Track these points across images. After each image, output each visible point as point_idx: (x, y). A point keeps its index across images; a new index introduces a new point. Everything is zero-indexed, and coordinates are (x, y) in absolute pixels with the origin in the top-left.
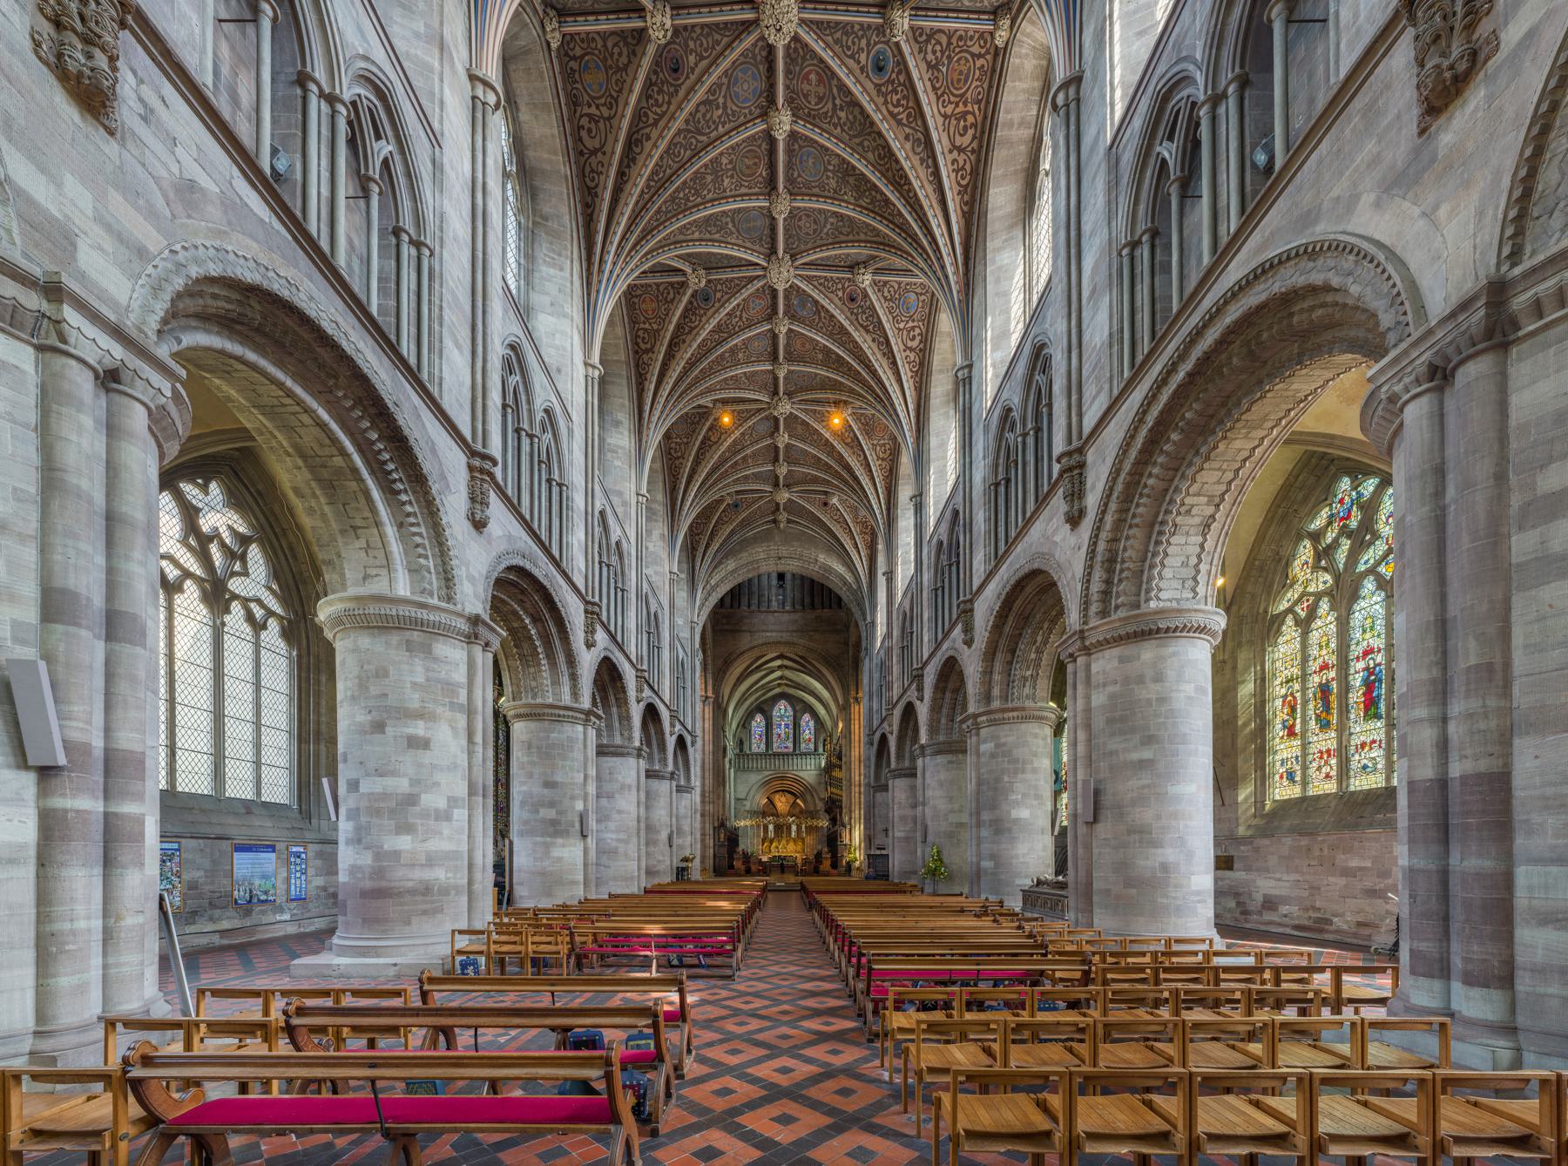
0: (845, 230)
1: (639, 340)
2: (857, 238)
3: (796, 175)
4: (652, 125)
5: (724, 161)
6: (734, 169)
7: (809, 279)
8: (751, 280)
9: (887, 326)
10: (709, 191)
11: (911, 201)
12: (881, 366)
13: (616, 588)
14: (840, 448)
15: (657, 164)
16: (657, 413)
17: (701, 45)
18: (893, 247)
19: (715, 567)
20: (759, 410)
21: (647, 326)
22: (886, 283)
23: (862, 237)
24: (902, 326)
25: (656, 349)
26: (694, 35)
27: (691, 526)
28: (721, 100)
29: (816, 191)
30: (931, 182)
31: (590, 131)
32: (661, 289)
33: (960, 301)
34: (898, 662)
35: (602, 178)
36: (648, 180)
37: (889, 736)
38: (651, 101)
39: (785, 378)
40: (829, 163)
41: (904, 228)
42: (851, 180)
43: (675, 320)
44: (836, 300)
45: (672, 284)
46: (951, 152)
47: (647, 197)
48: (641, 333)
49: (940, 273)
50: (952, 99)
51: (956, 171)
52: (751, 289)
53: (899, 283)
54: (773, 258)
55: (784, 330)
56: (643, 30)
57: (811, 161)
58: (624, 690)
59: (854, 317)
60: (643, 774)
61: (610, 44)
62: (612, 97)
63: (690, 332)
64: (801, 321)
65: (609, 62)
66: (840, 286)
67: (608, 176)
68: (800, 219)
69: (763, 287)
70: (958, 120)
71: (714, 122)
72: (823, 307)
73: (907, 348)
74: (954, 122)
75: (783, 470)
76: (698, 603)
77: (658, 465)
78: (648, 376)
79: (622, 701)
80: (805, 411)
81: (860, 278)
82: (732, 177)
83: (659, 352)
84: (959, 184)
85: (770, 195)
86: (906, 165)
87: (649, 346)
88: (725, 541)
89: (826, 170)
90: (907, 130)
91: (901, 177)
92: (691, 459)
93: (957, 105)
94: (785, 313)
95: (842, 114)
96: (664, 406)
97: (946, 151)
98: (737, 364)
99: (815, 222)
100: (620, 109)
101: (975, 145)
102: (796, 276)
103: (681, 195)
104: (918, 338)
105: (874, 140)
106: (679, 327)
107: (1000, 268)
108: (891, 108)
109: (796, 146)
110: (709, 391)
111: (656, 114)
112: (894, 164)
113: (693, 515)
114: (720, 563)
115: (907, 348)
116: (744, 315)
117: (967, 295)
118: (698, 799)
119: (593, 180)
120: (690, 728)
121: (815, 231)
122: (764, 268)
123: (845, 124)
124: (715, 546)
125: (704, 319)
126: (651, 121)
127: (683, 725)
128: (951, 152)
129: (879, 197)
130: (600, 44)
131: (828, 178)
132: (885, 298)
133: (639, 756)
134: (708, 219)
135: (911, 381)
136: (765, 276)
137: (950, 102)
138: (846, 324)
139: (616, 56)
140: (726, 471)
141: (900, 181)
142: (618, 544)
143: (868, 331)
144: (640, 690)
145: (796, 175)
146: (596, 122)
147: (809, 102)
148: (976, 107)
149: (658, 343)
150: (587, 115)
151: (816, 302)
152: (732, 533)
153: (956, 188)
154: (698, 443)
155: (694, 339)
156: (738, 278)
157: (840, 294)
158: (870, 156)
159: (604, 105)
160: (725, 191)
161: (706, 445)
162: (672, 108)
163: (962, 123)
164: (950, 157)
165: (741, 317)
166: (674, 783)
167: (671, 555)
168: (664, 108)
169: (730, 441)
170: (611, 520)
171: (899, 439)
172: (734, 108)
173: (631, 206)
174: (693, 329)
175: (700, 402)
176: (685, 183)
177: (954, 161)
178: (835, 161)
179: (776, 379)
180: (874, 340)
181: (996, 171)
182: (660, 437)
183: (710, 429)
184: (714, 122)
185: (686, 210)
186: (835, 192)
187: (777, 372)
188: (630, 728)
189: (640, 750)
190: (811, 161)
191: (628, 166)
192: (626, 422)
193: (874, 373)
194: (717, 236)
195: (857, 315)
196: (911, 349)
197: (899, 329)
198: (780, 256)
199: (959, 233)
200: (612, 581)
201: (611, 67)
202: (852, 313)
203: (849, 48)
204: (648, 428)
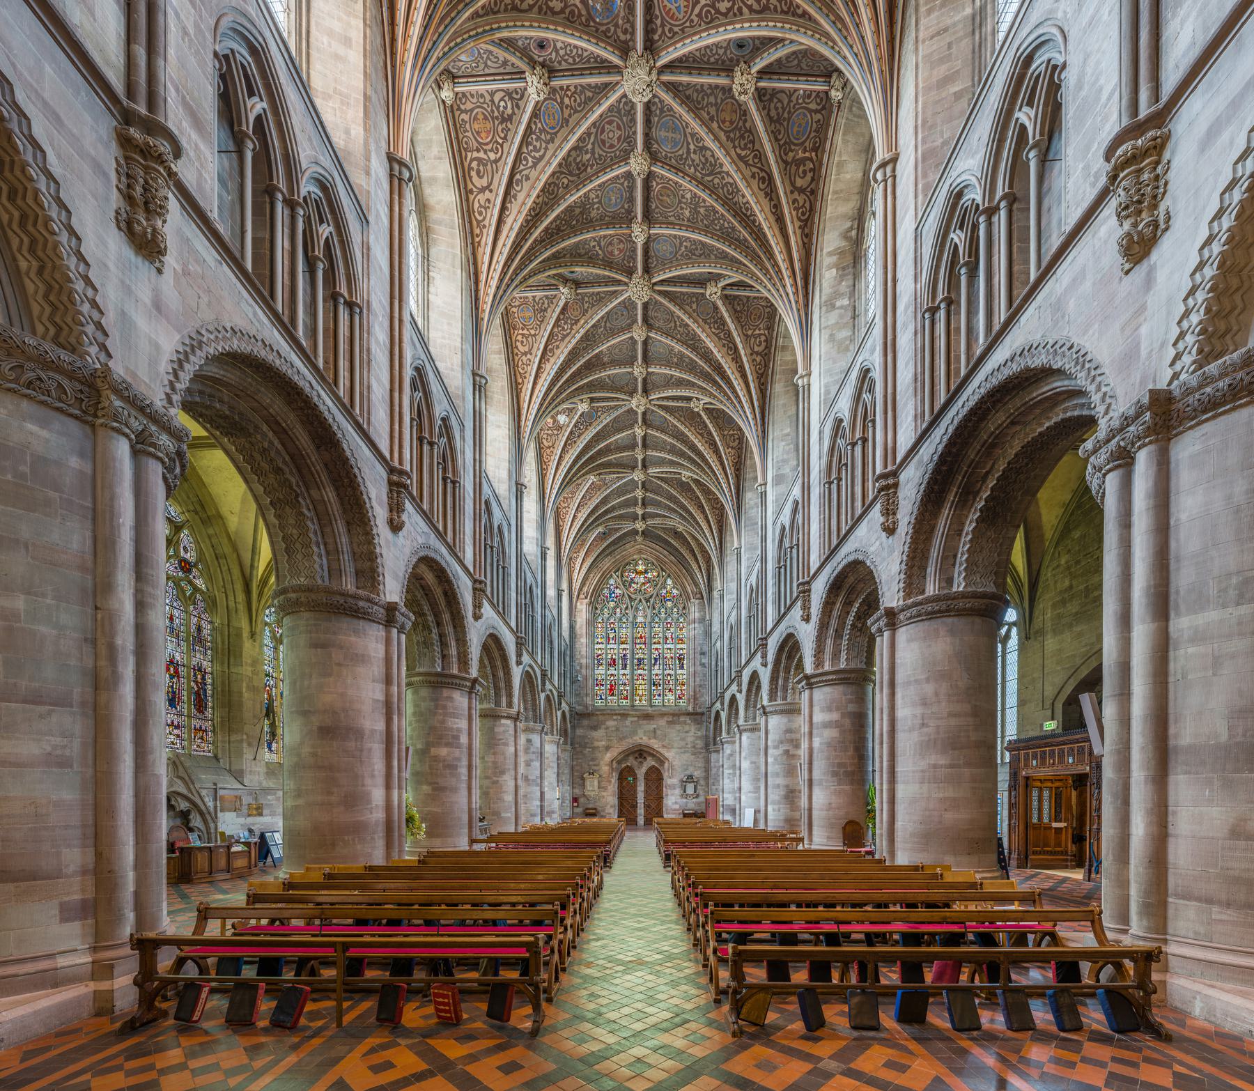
21: (525, 332)
24: (750, 332)
31: (478, 172)
38: (531, 148)
45: (547, 297)
48: (519, 338)
61: (496, 99)
63: (563, 339)
70: (798, 166)
74: (794, 168)
84: (799, 219)
104: (764, 344)
111: (534, 157)
128: (792, 192)
130: (488, 98)
150: (476, 159)
157: (694, 306)
159: (491, 150)
168: (541, 153)
177: (795, 201)
196: (758, 353)
197: (747, 336)
199: (800, 260)
201: (497, 118)
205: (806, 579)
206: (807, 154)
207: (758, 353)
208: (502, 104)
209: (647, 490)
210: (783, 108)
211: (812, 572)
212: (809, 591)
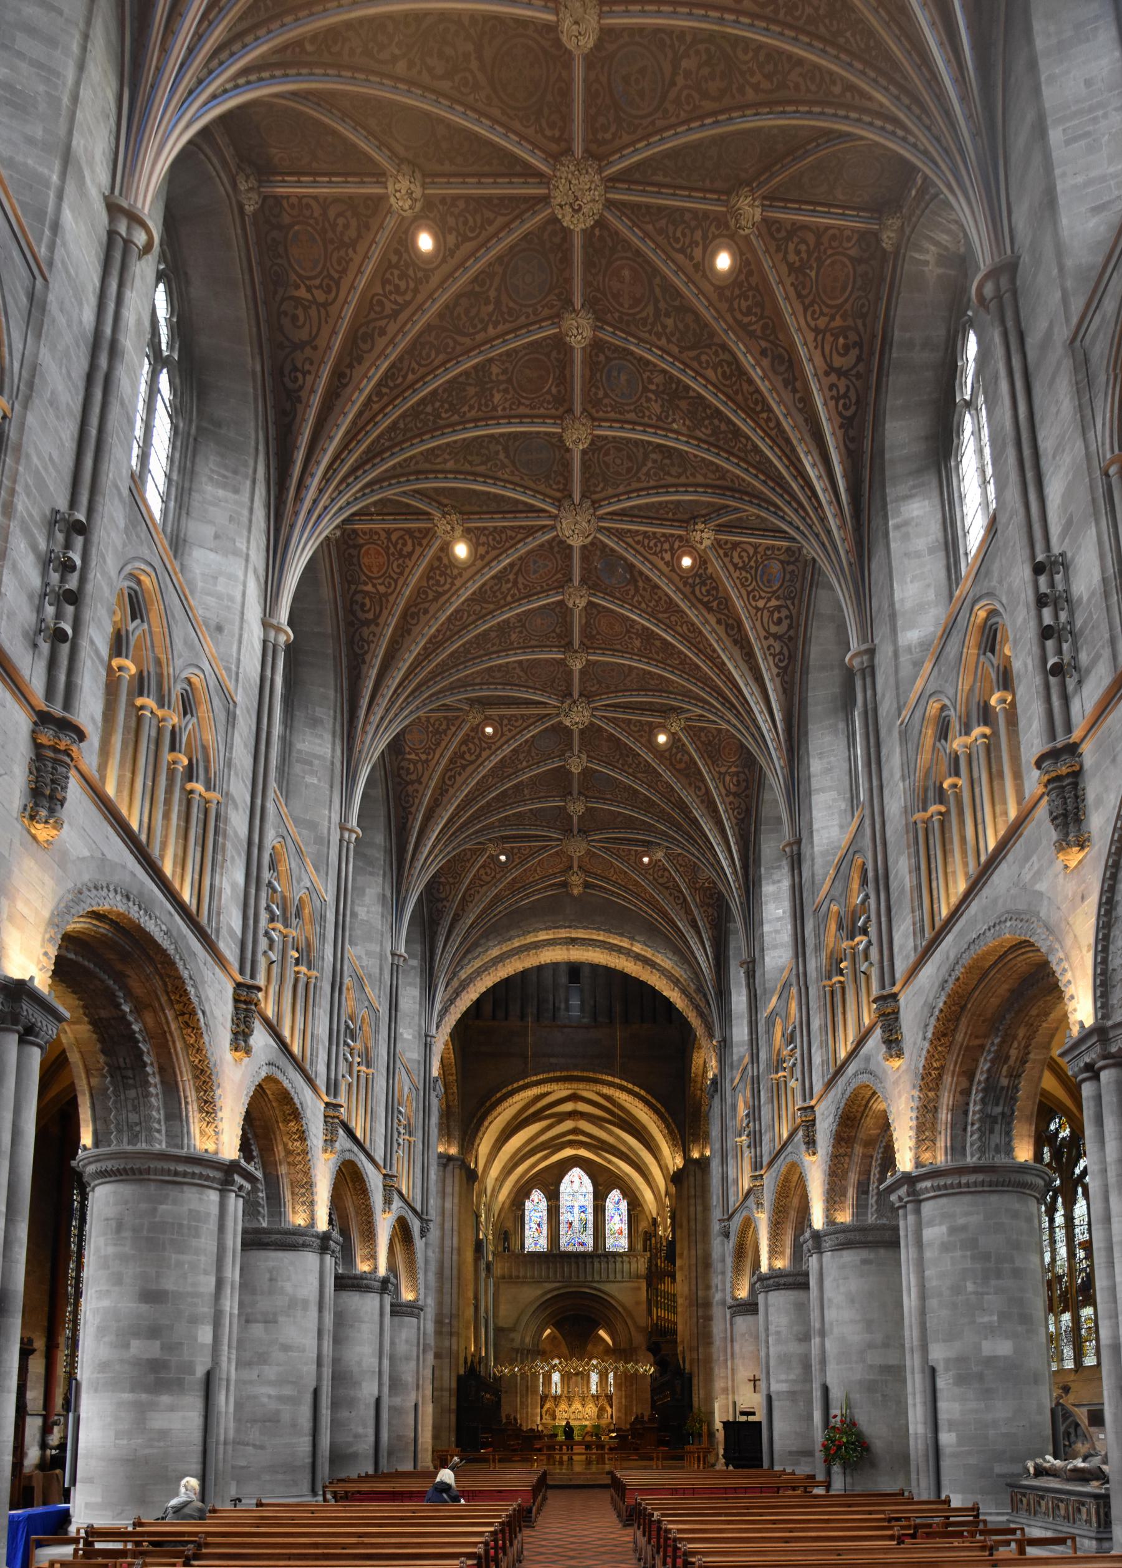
0: (674, 471)
1: (356, 607)
2: (692, 480)
3: (601, 394)
4: (389, 317)
5: (495, 370)
6: (509, 381)
7: (619, 535)
8: (532, 531)
9: (738, 604)
10: (471, 408)
11: (773, 433)
12: (731, 658)
14: (667, 776)
15: (393, 366)
16: (379, 712)
17: (466, 223)
18: (747, 493)
19: (468, 951)
20: (542, 718)
22: (735, 545)
23: (700, 479)
25: (381, 620)
26: (456, 211)
27: (429, 886)
28: (492, 294)
29: (631, 416)
30: (800, 410)
32: (394, 537)
33: (850, 564)
35: (309, 379)
36: (379, 384)
38: (388, 288)
39: (583, 672)
40: (650, 381)
41: (764, 468)
42: (683, 405)
43: (413, 580)
44: (661, 565)
45: (409, 531)
46: (827, 374)
47: (376, 407)
49: (818, 528)
50: (825, 310)
51: (837, 399)
52: (532, 543)
53: (756, 547)
54: (566, 503)
55: (582, 603)
56: (382, 199)
57: (623, 378)
59: (687, 590)
61: (332, 213)
62: (332, 278)
63: (436, 599)
64: (608, 593)
65: (330, 235)
66: (666, 546)
67: (317, 376)
68: (607, 454)
69: (550, 542)
70: (836, 337)
71: (482, 321)
72: (641, 573)
73: (769, 635)
74: (829, 338)
75: (577, 808)
76: (438, 1007)
77: (379, 792)
78: (368, 658)
80: (613, 720)
81: (697, 536)
82: (506, 391)
83: (386, 624)
84: (840, 414)
85: (561, 418)
86: (764, 386)
87: (370, 616)
88: (484, 911)
89: (646, 389)
90: (764, 344)
91: (756, 403)
92: (433, 784)
93: (833, 318)
94: (583, 581)
95: (669, 322)
96: (392, 702)
97: (820, 373)
98: (508, 649)
99: (629, 458)
100: (342, 295)
101: (861, 368)
102: (600, 529)
103: (429, 409)
104: (786, 623)
105: (716, 354)
106: (419, 591)
107: (906, 523)
108: (739, 316)
109: (602, 358)
110: (463, 684)
111: (396, 302)
112: (745, 386)
113: (432, 871)
114: (476, 945)
115: (769, 635)
116: (520, 580)
117: (860, 556)
118: (430, 1327)
119: (296, 380)
120: (419, 1208)
121: (629, 470)
122: (555, 517)
123: (673, 334)
125: (458, 583)
126: (388, 311)
128: (827, 374)
129: (723, 427)
130: (317, 212)
131: (648, 400)
132: (735, 566)
134: (467, 444)
135: (778, 680)
136: (553, 527)
137: (822, 314)
138: (677, 598)
139: (339, 229)
140: (488, 804)
141: (756, 407)
143: (710, 609)
145: (601, 394)
146: (306, 309)
147: (622, 305)
148: (859, 322)
149: (385, 612)
151: (631, 567)
153: (838, 420)
154: (444, 762)
155: (441, 608)
156: (512, 528)
157: (667, 556)
158: (710, 373)
159: (320, 287)
160: (495, 408)
161: (458, 764)
162: (420, 298)
163: (841, 340)
164: (826, 381)
165: (515, 582)
167: (395, 929)
169: (495, 760)
171: (762, 761)
172: (511, 304)
173: (350, 417)
174: (439, 595)
175: (447, 701)
176: (434, 393)
177: (832, 387)
178: (659, 379)
179: (570, 673)
180: (719, 622)
181: (893, 401)
182: (382, 746)
183: (464, 742)
184: (482, 321)
185: (436, 429)
186: (659, 418)
187: (570, 662)
190: (623, 378)
191: (351, 366)
192: (329, 724)
193: (721, 667)
194: (481, 469)
195: (693, 586)
196: (776, 637)
198: (577, 499)
201: (332, 241)
202: (685, 584)
203: (677, 240)
204: (364, 732)
206: (850, 322)
207: (776, 637)
208: (341, 221)
209: (588, 873)
210: (808, 251)
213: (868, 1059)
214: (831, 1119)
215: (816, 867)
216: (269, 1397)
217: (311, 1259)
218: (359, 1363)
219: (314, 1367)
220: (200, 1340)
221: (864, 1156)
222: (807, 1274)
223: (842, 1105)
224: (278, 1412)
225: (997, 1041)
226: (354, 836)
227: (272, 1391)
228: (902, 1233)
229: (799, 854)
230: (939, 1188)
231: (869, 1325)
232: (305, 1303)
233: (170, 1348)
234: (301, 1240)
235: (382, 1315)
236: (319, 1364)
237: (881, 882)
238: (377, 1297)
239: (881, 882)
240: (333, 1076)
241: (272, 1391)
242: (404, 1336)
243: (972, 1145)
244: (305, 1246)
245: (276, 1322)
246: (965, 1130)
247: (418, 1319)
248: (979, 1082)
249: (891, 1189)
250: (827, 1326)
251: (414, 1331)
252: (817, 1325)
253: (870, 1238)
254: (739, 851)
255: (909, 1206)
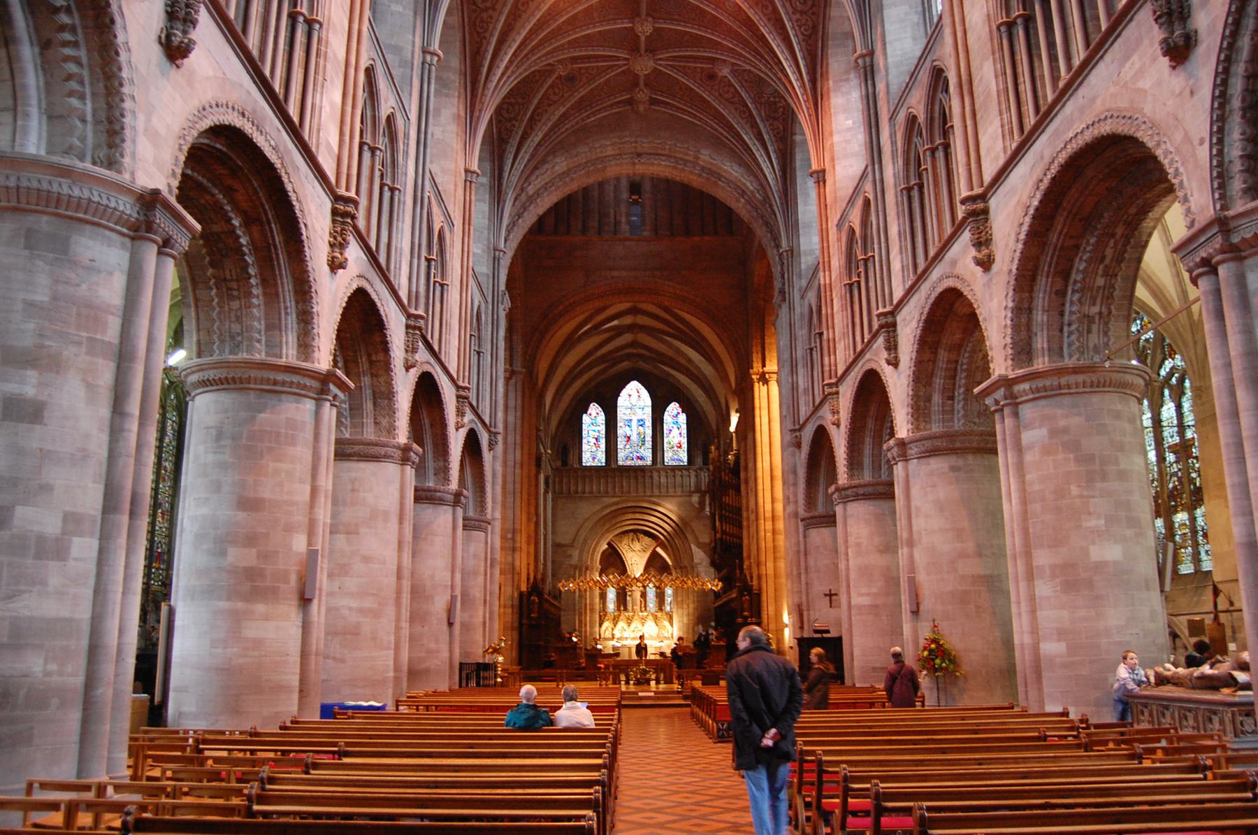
13: (382, 186)
34: (844, 308)
37: (832, 430)
58: (385, 347)
60: (410, 495)
79: (382, 366)
124: (537, 137)
127: (475, 411)
133: (405, 460)
142: (390, 120)
144: (411, 349)
152: (564, 117)
166: (460, 512)
170: (382, 84)
188: (392, 411)
189: (406, 449)
200: (377, 174)
205: (978, 191)
211: (987, 178)
212: (986, 211)
213: (954, 263)
214: (914, 324)
215: (890, 77)
216: (350, 609)
217: (391, 470)
218: (432, 577)
219: (395, 579)
220: (295, 548)
221: (949, 362)
222: (891, 484)
223: (926, 310)
224: (358, 625)
225: (1092, 241)
226: (436, 58)
227: (354, 604)
228: (999, 437)
229: (872, 66)
230: (1038, 390)
231: (959, 534)
232: (386, 515)
233: (265, 556)
234: (383, 451)
235: (454, 528)
236: (399, 577)
237: (965, 88)
238: (450, 509)
239: (965, 88)
240: (414, 289)
241: (354, 604)
242: (472, 549)
243: (1070, 345)
244: (386, 456)
245: (358, 534)
246: (1061, 331)
247: (486, 533)
248: (1075, 281)
249: (986, 393)
250: (915, 536)
251: (482, 545)
252: (905, 535)
253: (958, 445)
254: (808, 73)
255: (1007, 411)
